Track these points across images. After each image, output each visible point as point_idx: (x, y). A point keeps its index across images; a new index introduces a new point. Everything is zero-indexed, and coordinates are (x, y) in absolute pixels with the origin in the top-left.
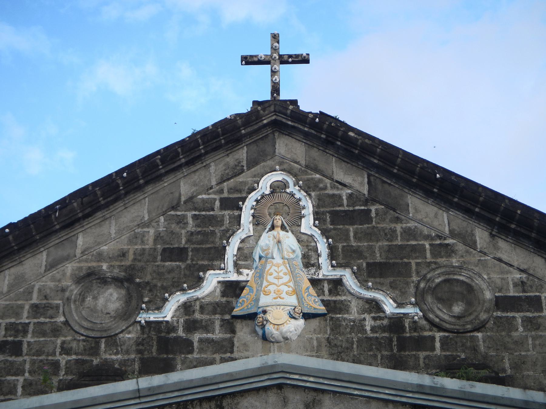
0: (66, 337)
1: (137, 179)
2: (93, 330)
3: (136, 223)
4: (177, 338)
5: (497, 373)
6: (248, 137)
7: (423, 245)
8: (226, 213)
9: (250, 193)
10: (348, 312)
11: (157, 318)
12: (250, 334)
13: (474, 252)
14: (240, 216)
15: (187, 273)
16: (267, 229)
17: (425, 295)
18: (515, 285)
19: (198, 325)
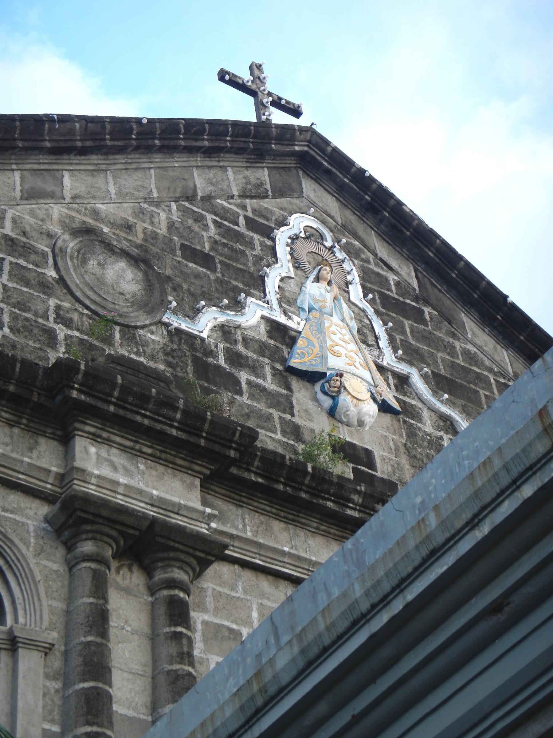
4: (218, 368)
6: (272, 157)
12: (312, 401)
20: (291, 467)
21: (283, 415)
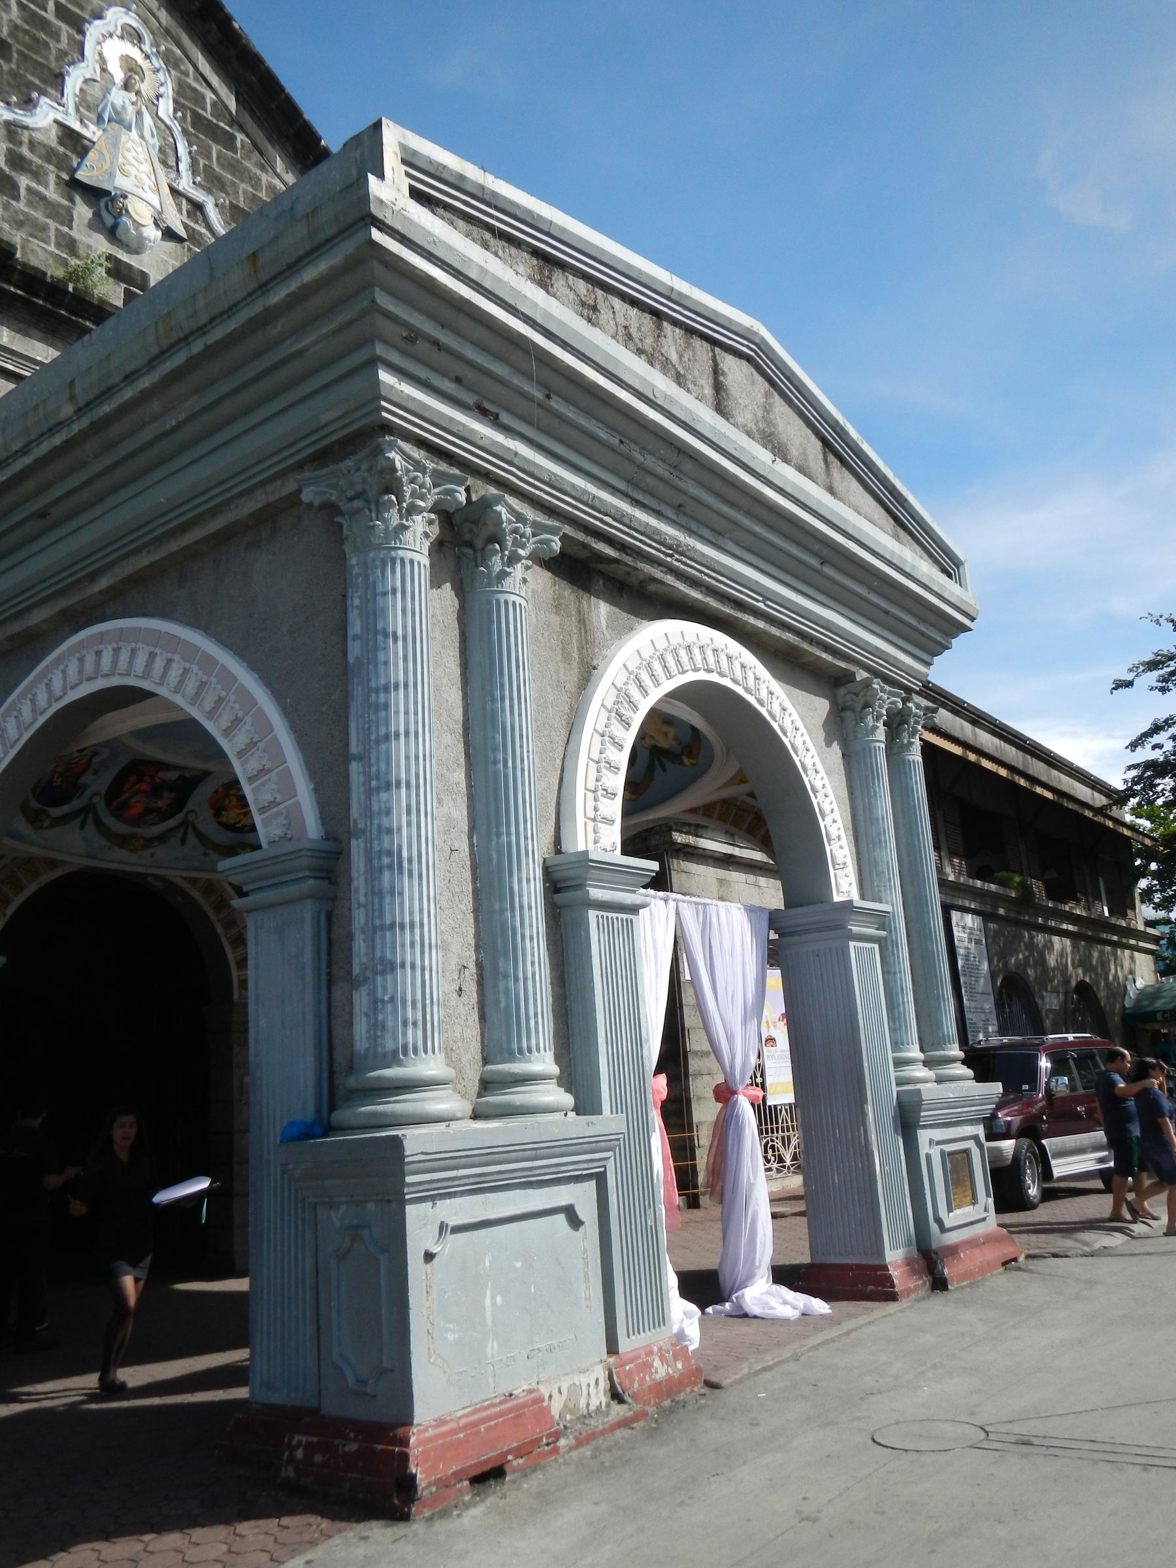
19: (25, 165)
20: (51, 285)
21: (60, 227)
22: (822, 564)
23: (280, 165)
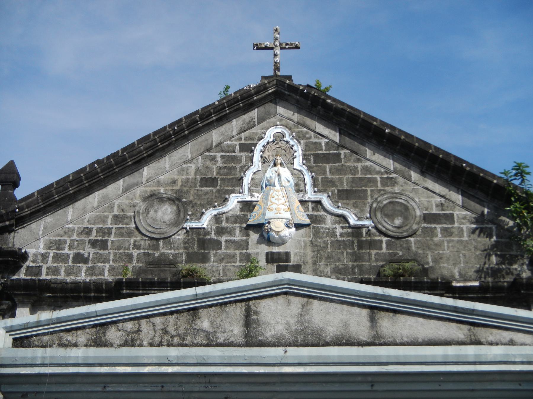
0: (137, 237)
1: (183, 130)
2: (155, 233)
3: (182, 161)
4: (211, 240)
5: (423, 266)
7: (376, 178)
8: (244, 154)
9: (259, 140)
10: (325, 223)
11: (198, 225)
13: (410, 183)
14: (253, 157)
15: (217, 195)
16: (271, 166)
17: (377, 212)
18: (437, 206)
19: (224, 231)
21: (242, 251)
22: (372, 386)
23: (369, 153)
